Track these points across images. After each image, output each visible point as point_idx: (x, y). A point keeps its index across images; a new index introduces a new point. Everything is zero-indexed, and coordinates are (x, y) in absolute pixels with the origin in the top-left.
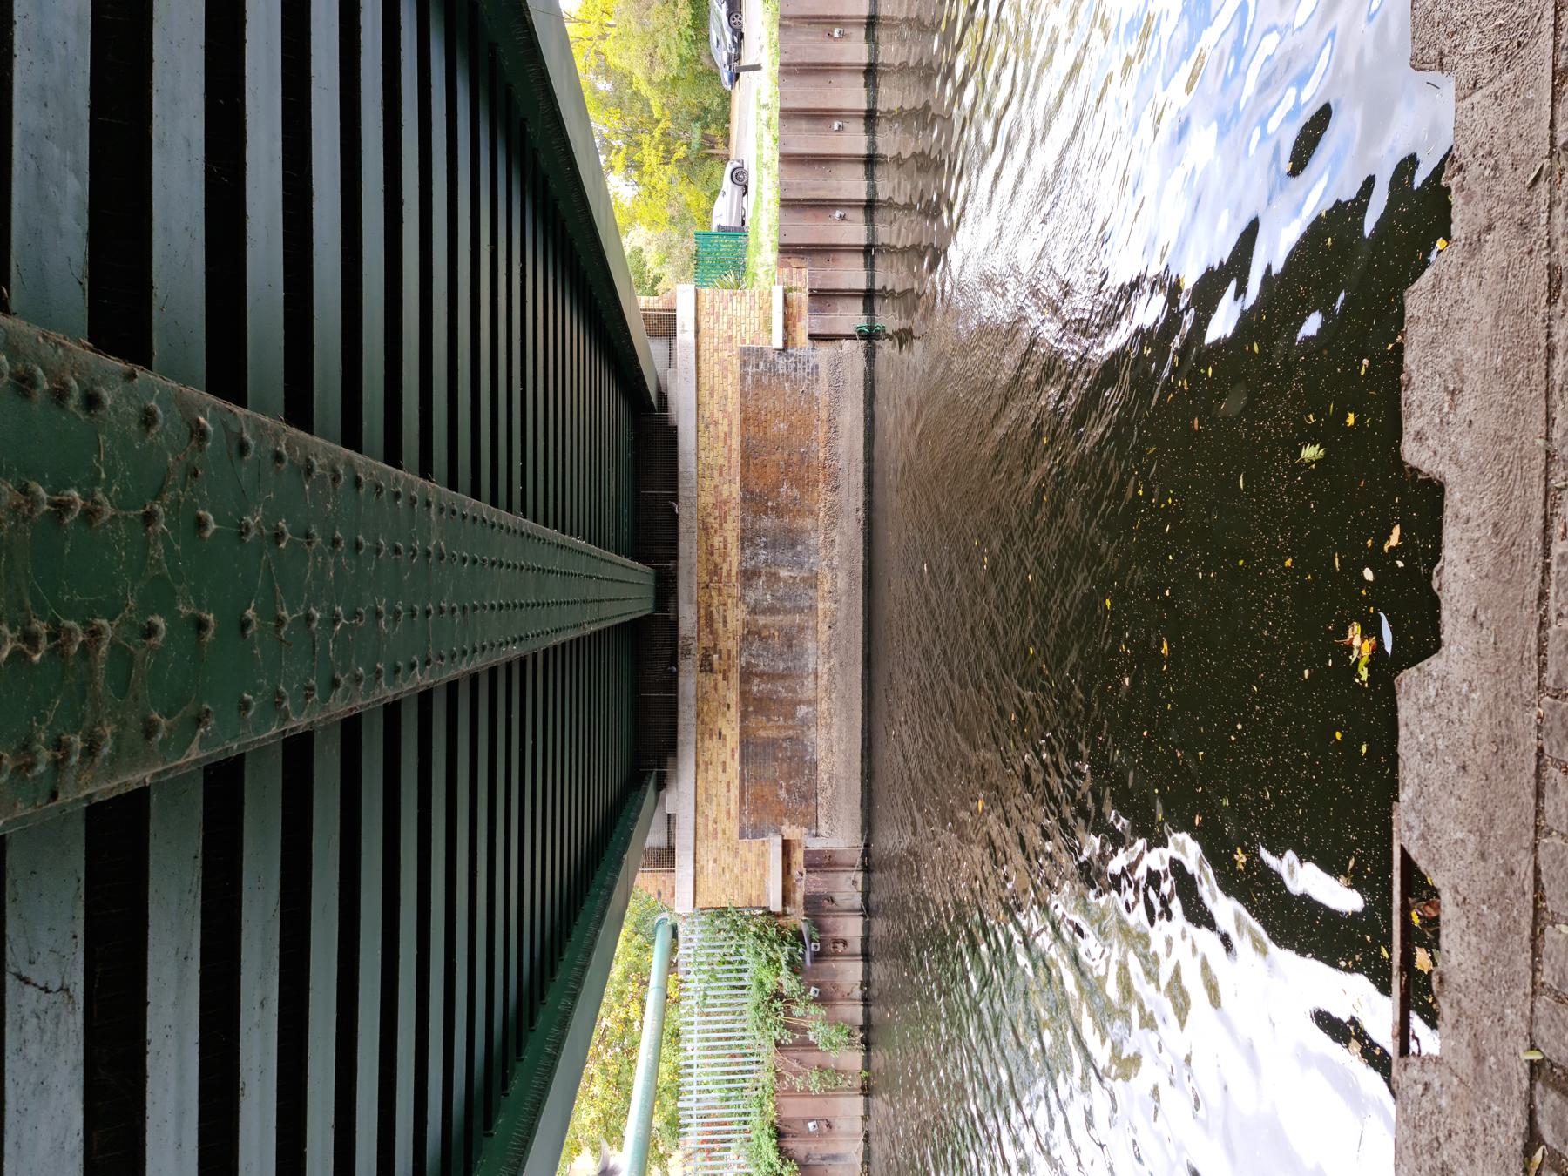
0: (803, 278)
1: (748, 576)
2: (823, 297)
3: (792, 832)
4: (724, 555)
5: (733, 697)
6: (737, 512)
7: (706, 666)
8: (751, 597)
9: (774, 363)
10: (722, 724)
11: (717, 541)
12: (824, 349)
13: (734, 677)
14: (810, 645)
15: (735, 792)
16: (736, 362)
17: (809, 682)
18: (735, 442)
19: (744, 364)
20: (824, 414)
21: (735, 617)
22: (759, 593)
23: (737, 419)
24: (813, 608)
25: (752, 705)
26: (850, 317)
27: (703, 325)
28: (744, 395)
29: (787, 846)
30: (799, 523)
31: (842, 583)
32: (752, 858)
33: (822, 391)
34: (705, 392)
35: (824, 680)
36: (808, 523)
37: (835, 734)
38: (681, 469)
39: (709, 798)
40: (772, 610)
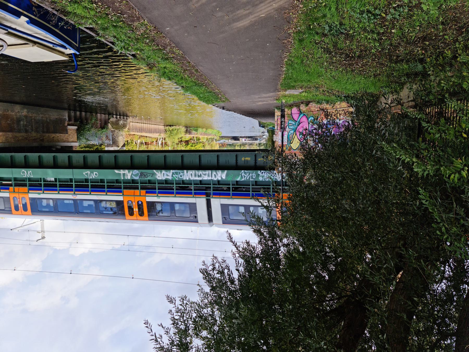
1: (26, 131)
3: (66, 125)
4: (23, 136)
5: (47, 135)
7: (42, 140)
8: (30, 130)
10: (51, 137)
11: (20, 138)
13: (44, 134)
14: (38, 118)
15: (61, 135)
17: (43, 118)
21: (34, 134)
22: (29, 128)
24: (31, 117)
25: (48, 132)
29: (69, 125)
30: (15, 119)
32: (70, 132)
35: (43, 116)
37: (51, 114)
38: (8, 146)
39: (63, 140)
40: (32, 126)
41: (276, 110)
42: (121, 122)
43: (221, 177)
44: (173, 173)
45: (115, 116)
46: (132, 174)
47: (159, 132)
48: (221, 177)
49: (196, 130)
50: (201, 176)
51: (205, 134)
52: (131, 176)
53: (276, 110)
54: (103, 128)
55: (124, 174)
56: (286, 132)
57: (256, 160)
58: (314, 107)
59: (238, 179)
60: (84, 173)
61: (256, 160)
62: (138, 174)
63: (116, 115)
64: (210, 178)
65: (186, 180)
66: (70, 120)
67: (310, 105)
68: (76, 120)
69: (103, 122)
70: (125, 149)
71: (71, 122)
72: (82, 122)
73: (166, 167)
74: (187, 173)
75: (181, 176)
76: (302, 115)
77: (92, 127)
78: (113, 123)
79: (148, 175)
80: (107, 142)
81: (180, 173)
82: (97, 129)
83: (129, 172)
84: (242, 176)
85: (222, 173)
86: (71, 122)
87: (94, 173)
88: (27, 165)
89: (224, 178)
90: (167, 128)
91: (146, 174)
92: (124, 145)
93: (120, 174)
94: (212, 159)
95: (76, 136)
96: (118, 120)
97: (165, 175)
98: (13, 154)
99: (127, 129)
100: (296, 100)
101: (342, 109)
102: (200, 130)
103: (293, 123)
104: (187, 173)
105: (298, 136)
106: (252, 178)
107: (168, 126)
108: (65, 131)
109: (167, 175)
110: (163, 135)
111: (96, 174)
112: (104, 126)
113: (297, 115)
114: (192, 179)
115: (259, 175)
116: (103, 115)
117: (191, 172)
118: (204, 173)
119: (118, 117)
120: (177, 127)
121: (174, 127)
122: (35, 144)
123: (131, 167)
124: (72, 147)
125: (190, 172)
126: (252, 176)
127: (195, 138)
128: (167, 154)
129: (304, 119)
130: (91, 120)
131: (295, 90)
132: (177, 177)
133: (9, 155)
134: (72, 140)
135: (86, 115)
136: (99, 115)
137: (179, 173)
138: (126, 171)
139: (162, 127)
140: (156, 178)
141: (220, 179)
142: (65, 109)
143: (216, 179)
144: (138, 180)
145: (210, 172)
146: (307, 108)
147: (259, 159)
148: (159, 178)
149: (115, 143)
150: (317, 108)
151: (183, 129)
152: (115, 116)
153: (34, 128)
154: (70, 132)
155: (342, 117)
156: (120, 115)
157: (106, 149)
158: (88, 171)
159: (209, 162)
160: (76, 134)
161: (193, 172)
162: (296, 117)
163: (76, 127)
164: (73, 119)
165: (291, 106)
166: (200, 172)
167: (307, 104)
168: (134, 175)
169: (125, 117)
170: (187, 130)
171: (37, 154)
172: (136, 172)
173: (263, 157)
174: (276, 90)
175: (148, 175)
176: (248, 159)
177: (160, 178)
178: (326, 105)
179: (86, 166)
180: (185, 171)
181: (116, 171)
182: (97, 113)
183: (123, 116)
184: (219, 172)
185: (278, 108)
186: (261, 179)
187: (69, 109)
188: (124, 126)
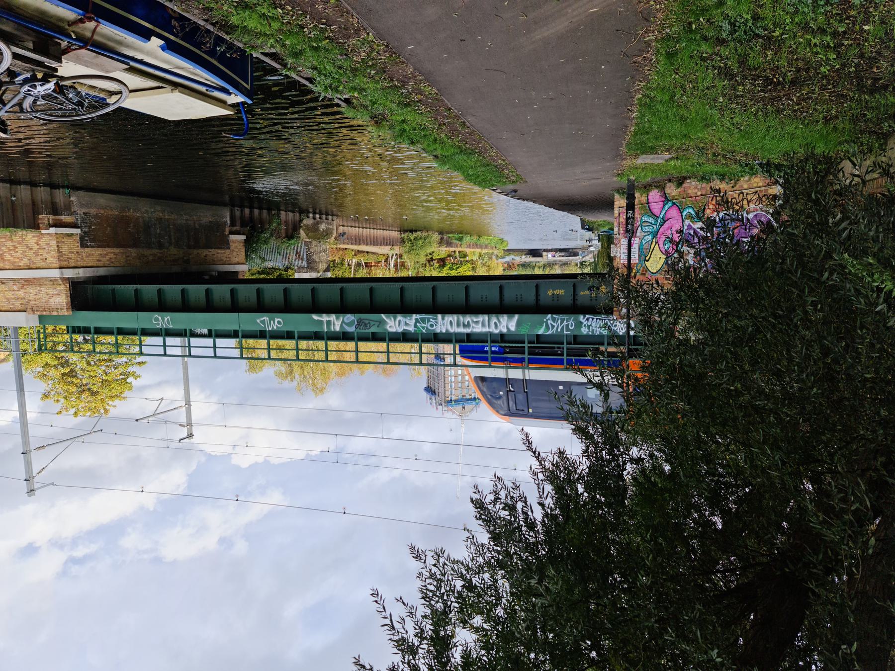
0: (44, 218)
1: (161, 246)
2: (54, 210)
3: (227, 233)
5: (195, 251)
6: (141, 250)
8: (167, 245)
9: (85, 233)
11: (151, 258)
12: (75, 208)
14: (179, 222)
15: (219, 251)
16: (87, 250)
17: (189, 222)
18: (117, 250)
19: (87, 247)
20: (102, 212)
21: (173, 251)
23: (109, 250)
25: (197, 246)
26: (60, 195)
27: (73, 265)
28: (99, 247)
29: (232, 233)
31: (159, 208)
32: (234, 245)
33: (93, 211)
34: (100, 264)
36: (141, 220)
39: (222, 260)
40: (170, 237)
41: (617, 196)
42: (323, 227)
43: (508, 328)
44: (417, 321)
45: (311, 215)
46: (343, 322)
47: (391, 242)
48: (508, 328)
49: (461, 239)
50: (468, 325)
51: (476, 246)
52: (341, 325)
53: (617, 196)
54: (290, 237)
55: (329, 322)
56: (637, 239)
57: (575, 294)
58: (693, 187)
59: (541, 331)
60: (258, 321)
61: (575, 294)
62: (353, 321)
63: (314, 213)
64: (486, 330)
65: (441, 333)
66: (233, 224)
67: (685, 185)
68: (243, 224)
69: (290, 227)
70: (329, 275)
71: (235, 228)
72: (253, 228)
73: (404, 308)
74: (443, 319)
75: (432, 326)
76: (669, 205)
77: (271, 235)
78: (308, 229)
79: (372, 323)
80: (298, 263)
81: (429, 321)
82: (279, 240)
83: (337, 318)
84: (547, 326)
85: (510, 318)
86: (235, 228)
87: (276, 320)
88: (162, 306)
89: (513, 329)
90: (405, 235)
91: (367, 322)
92: (328, 269)
93: (322, 321)
94: (491, 293)
95: (243, 254)
96: (318, 223)
97: (402, 323)
98: (139, 286)
99: (333, 238)
100: (658, 177)
101: (754, 190)
102: (467, 239)
103: (651, 220)
104: (443, 319)
105: (661, 245)
106: (568, 329)
107: (405, 231)
108: (225, 244)
109: (406, 324)
110: (397, 250)
111: (279, 322)
112: (292, 234)
113: (660, 205)
114: (451, 331)
115: (581, 323)
116: (291, 215)
117: (451, 319)
118: (475, 320)
119: (318, 216)
120: (424, 234)
121: (418, 233)
122: (176, 269)
123: (341, 308)
124: (236, 273)
125: (449, 318)
126: (567, 326)
127: (457, 254)
128: (406, 284)
129: (674, 212)
130: (270, 223)
131: (656, 156)
132: (423, 328)
133: (131, 288)
134: (236, 260)
135: (260, 214)
136: (283, 213)
137: (429, 319)
138: (333, 317)
139: (396, 234)
140: (386, 330)
141: (505, 330)
142: (224, 204)
143: (497, 332)
144: (353, 333)
145: (486, 317)
146: (679, 190)
147: (582, 293)
148: (390, 330)
149: (311, 266)
150: (701, 189)
151: (436, 237)
152: (311, 215)
153: (173, 241)
154: (233, 246)
155: (752, 206)
156: (321, 214)
157: (297, 276)
158: (265, 318)
159: (484, 299)
160: (243, 250)
161: (453, 318)
162: (656, 208)
163: (243, 237)
164: (238, 222)
165: (647, 188)
166: (468, 318)
167: (680, 182)
168: (346, 324)
169: (330, 217)
170: (442, 239)
171: (179, 287)
172: (350, 317)
173: (589, 289)
174: (618, 156)
175: (372, 323)
176: (561, 292)
177: (393, 330)
178: (719, 183)
179: (261, 307)
180: (440, 316)
181: (315, 317)
182: (279, 210)
183: (327, 214)
184: (504, 319)
185: (620, 191)
186: (584, 331)
187: (232, 205)
188: (327, 234)
